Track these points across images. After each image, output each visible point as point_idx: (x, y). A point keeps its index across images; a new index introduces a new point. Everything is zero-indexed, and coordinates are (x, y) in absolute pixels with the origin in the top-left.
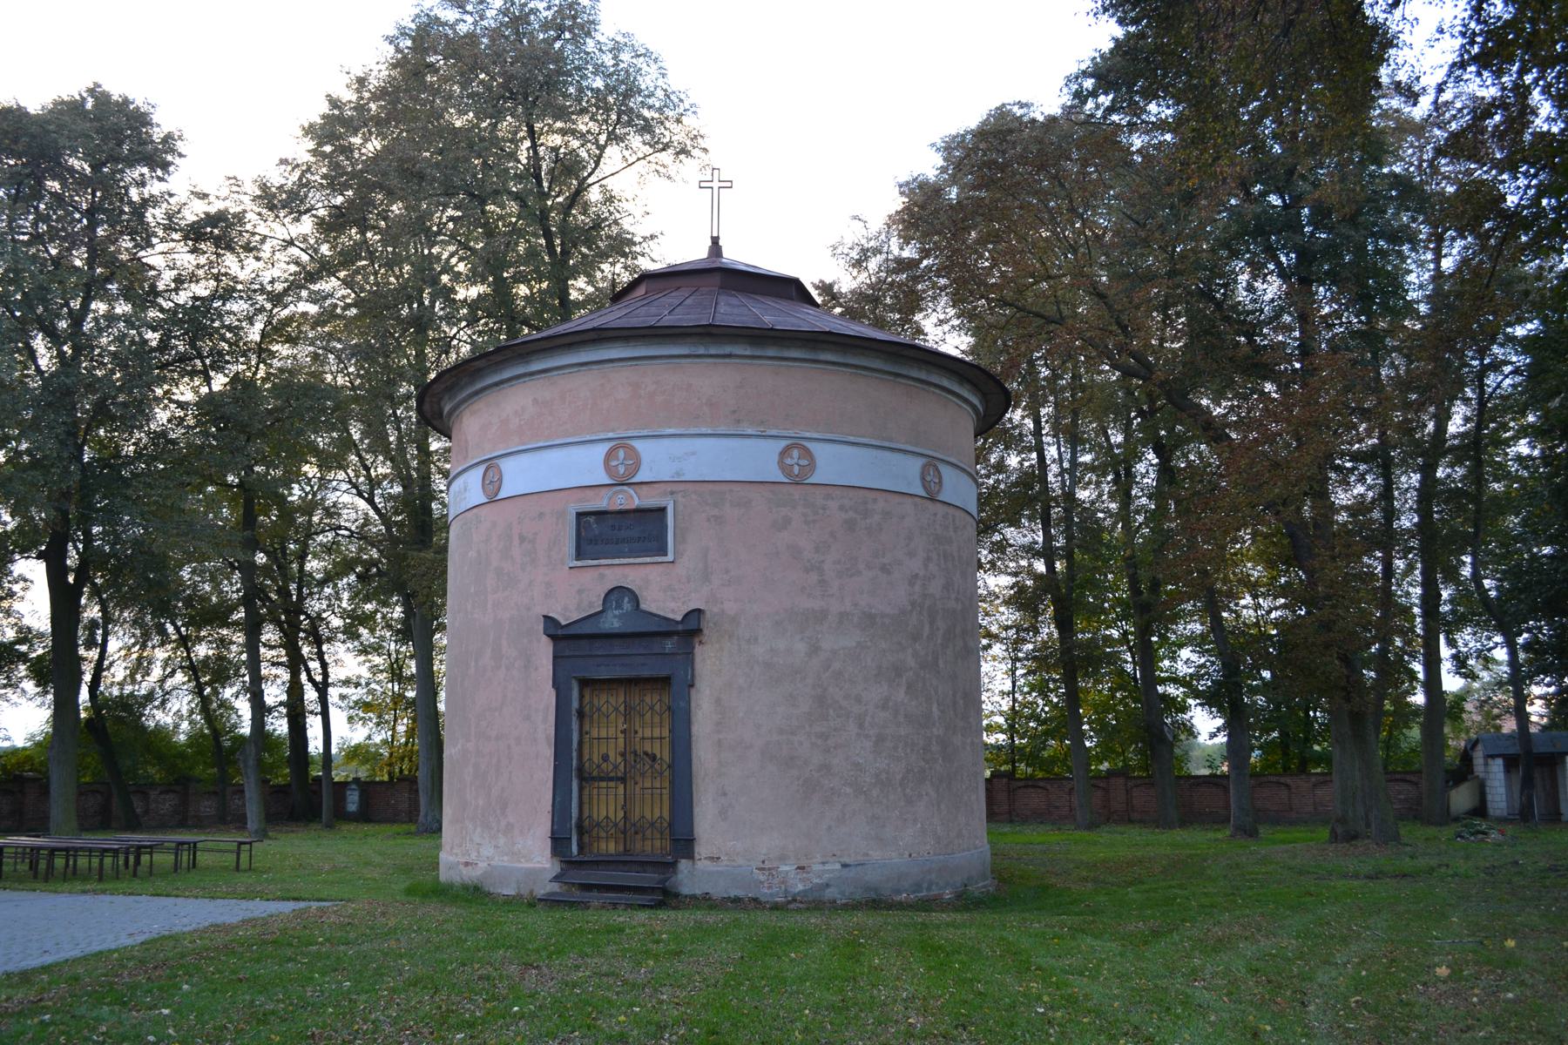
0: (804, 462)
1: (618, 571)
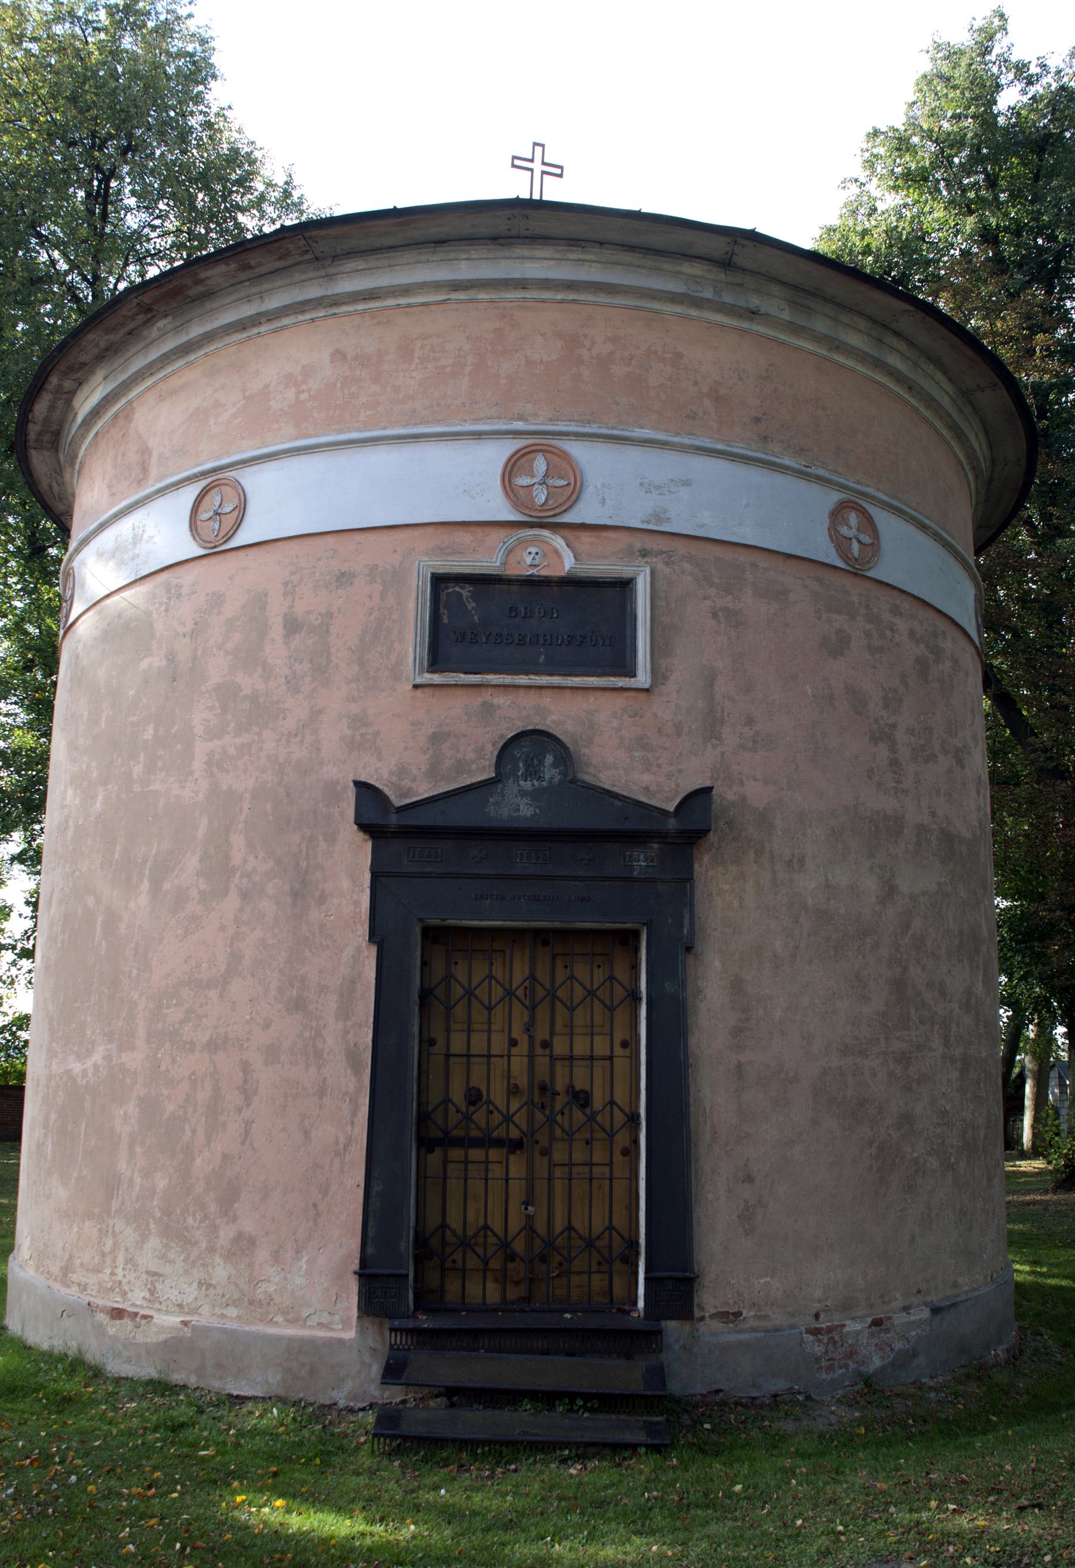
0: (866, 539)
1: (528, 700)
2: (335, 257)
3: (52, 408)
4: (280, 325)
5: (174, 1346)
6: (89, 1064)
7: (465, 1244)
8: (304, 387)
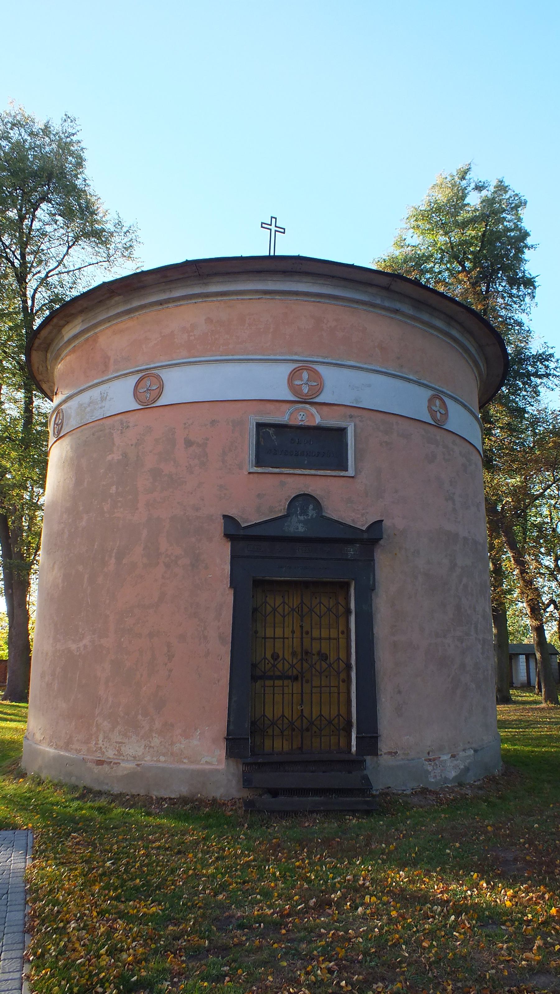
2: (208, 275)
3: (50, 333)
4: (179, 304)
5: (131, 776)
6: (81, 644)
7: (273, 723)
8: (191, 334)
